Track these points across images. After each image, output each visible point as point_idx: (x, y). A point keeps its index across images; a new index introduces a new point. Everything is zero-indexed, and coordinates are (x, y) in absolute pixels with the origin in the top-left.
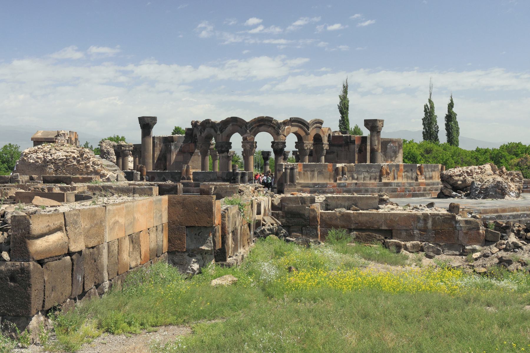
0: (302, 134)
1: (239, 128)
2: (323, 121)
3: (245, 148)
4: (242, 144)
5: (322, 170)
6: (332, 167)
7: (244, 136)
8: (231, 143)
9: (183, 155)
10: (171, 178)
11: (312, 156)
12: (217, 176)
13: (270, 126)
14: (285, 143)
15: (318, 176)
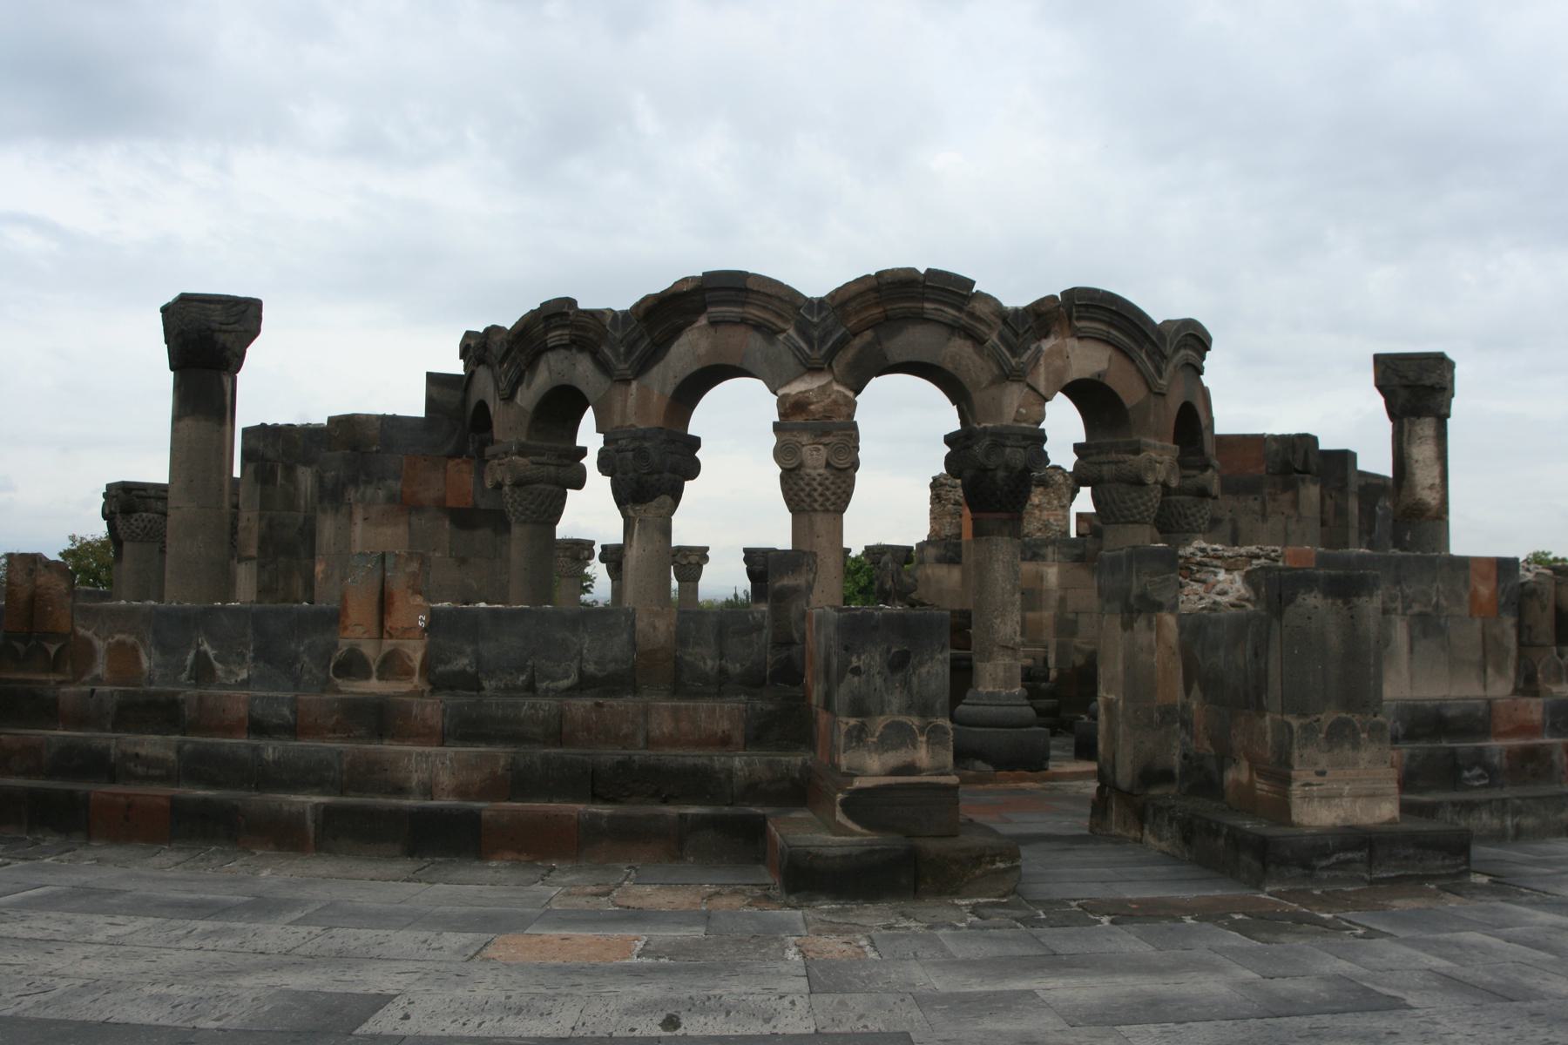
0: (1130, 390)
1: (755, 341)
2: (1210, 339)
3: (791, 464)
4: (772, 440)
5: (1437, 604)
6: (1493, 583)
7: (780, 392)
8: (695, 443)
9: (410, 525)
10: (254, 659)
11: (958, 563)
12: (633, 644)
13: (955, 329)
14: (1042, 438)
15: (1411, 650)
